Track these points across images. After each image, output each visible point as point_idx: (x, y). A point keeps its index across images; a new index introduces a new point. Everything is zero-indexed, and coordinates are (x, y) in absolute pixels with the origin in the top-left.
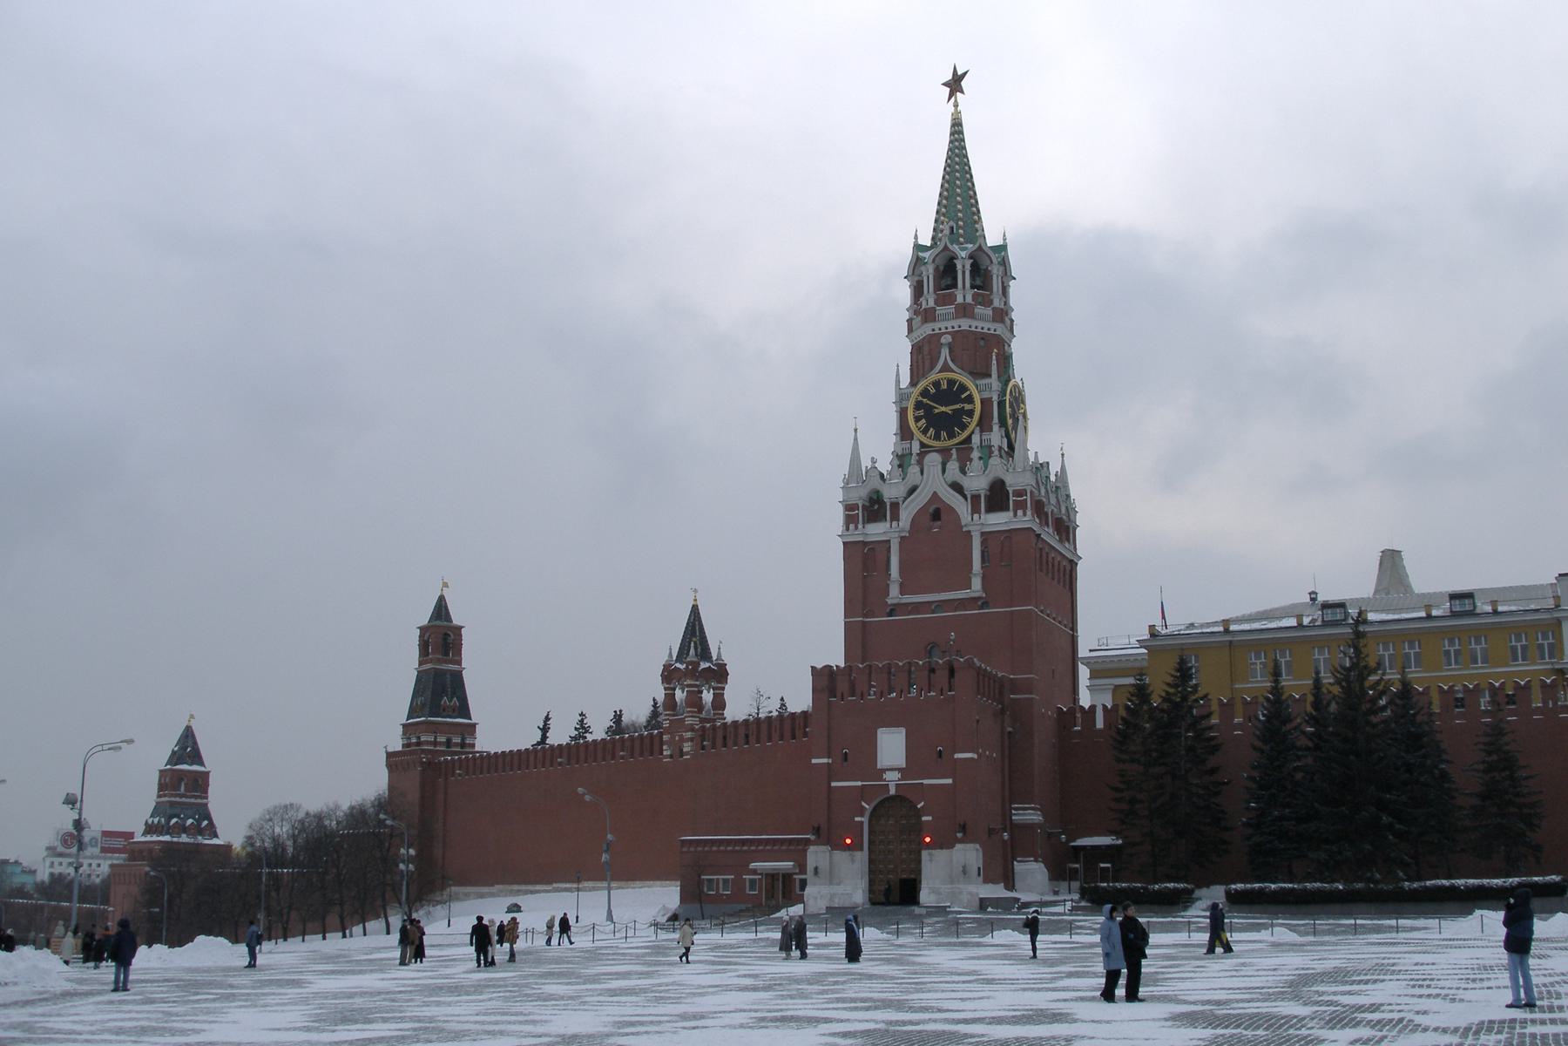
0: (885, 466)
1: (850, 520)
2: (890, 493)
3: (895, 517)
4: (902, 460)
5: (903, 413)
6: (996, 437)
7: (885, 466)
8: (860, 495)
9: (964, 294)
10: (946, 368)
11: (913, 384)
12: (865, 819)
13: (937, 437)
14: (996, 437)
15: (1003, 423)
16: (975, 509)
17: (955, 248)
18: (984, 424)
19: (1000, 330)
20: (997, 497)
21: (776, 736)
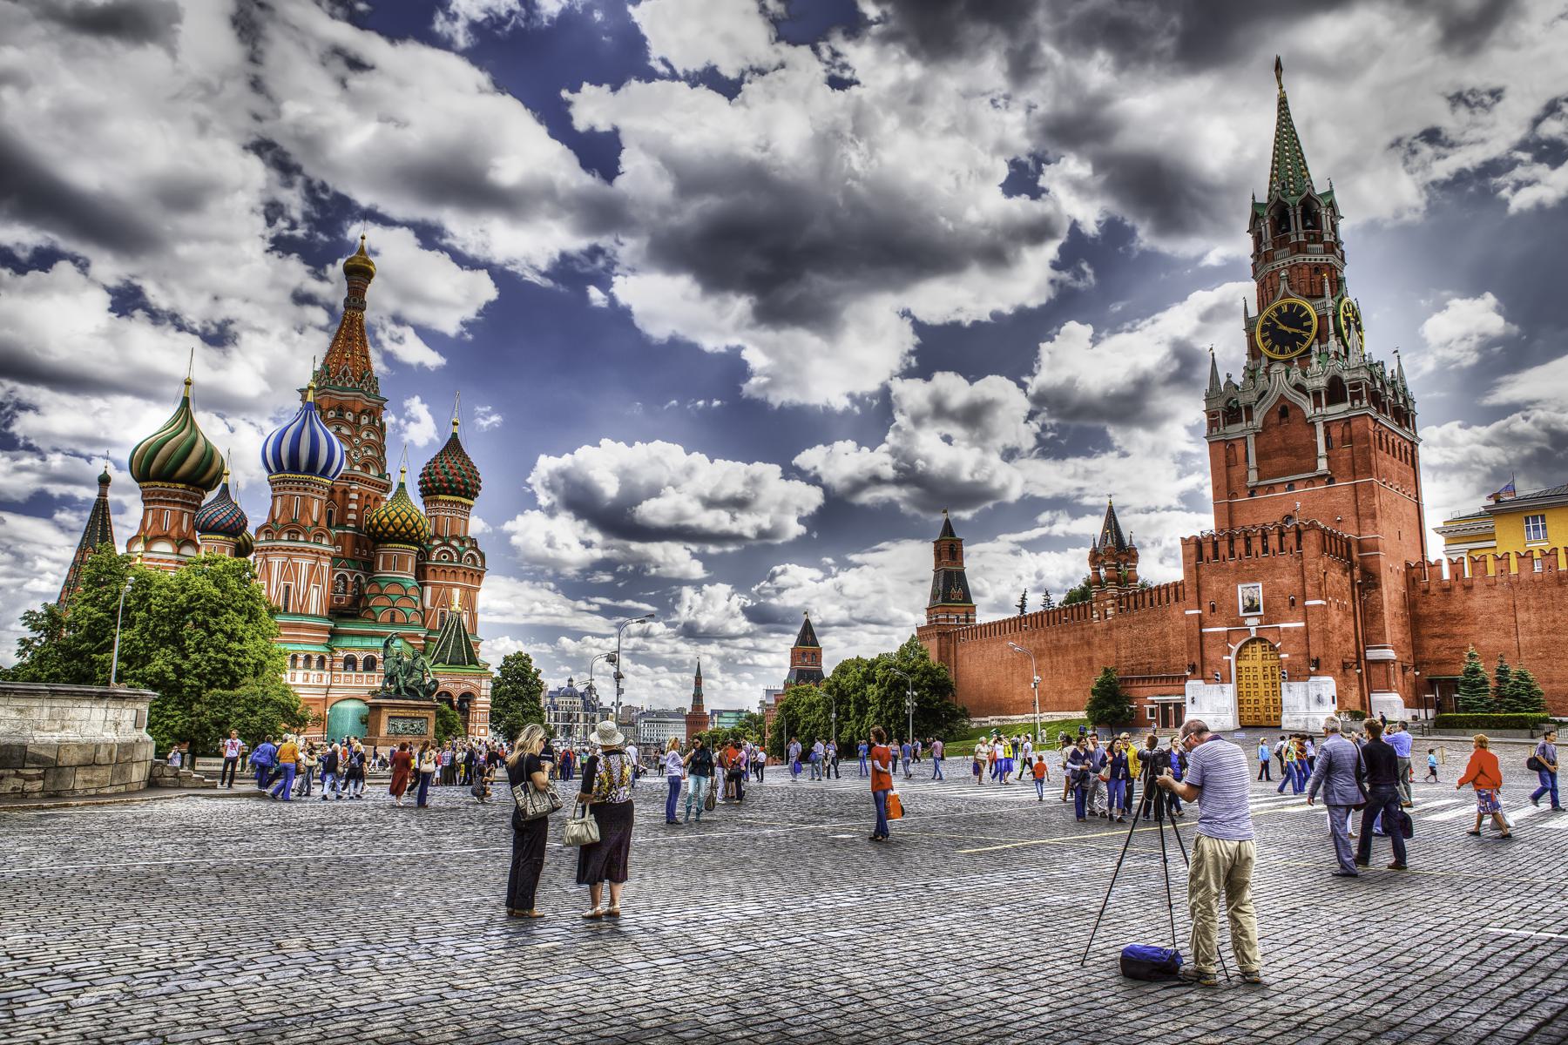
0: (1238, 379)
1: (1212, 424)
2: (1243, 400)
3: (1250, 418)
4: (1251, 373)
5: (1251, 337)
6: (1333, 344)
7: (1238, 379)
8: (1220, 404)
9: (1297, 235)
10: (1286, 296)
11: (1260, 313)
12: (1232, 658)
13: (1282, 352)
14: (1333, 344)
15: (1338, 333)
16: (1317, 404)
17: (1290, 201)
18: (1322, 336)
19: (1332, 259)
20: (1336, 391)
21: (1172, 598)
